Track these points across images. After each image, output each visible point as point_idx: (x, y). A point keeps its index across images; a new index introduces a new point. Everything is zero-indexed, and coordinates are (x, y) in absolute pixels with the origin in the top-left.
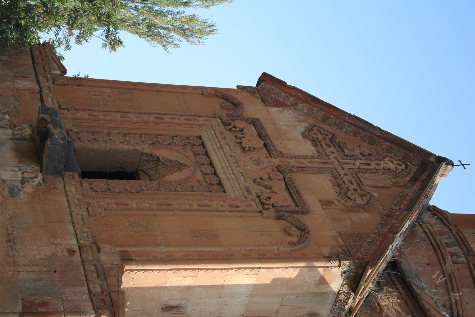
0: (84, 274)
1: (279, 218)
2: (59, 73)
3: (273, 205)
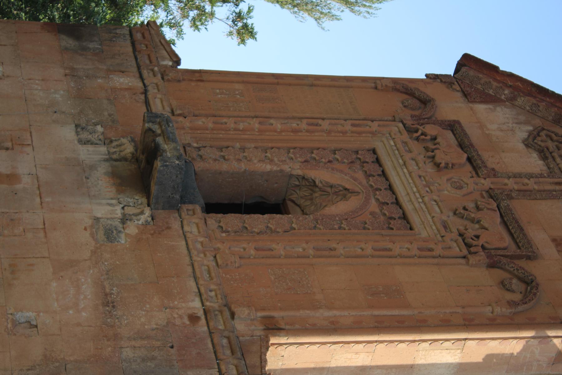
0: (212, 350)
1: (492, 266)
2: (170, 63)
3: (483, 247)
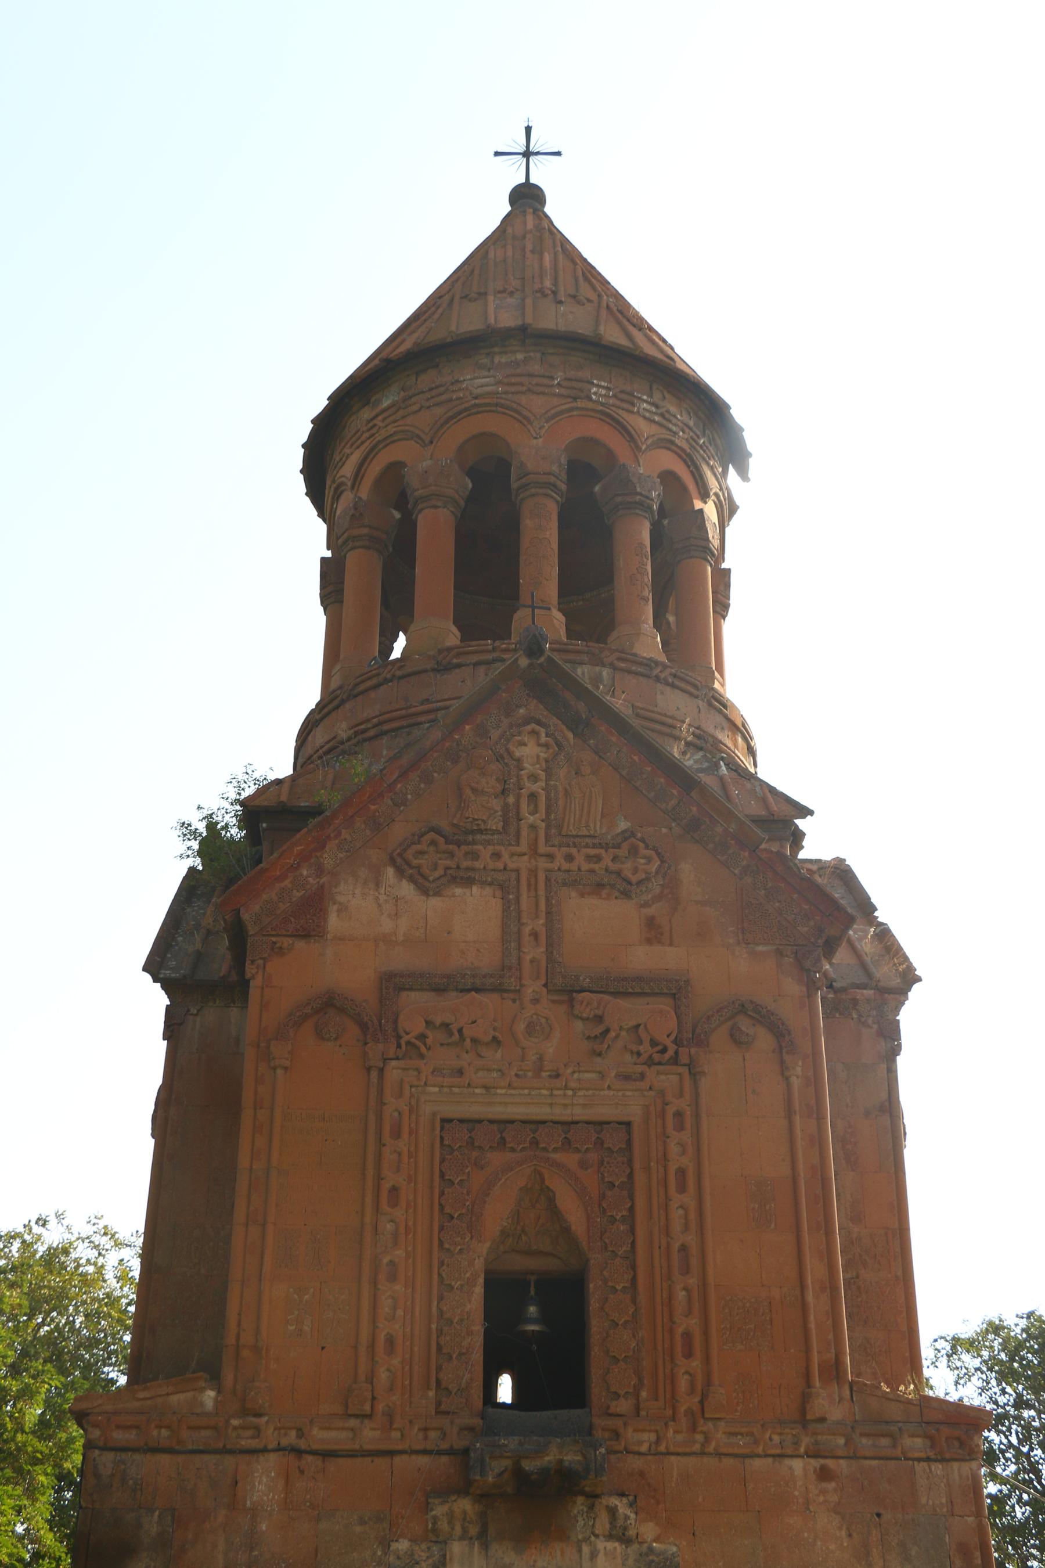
0: (882, 1462)
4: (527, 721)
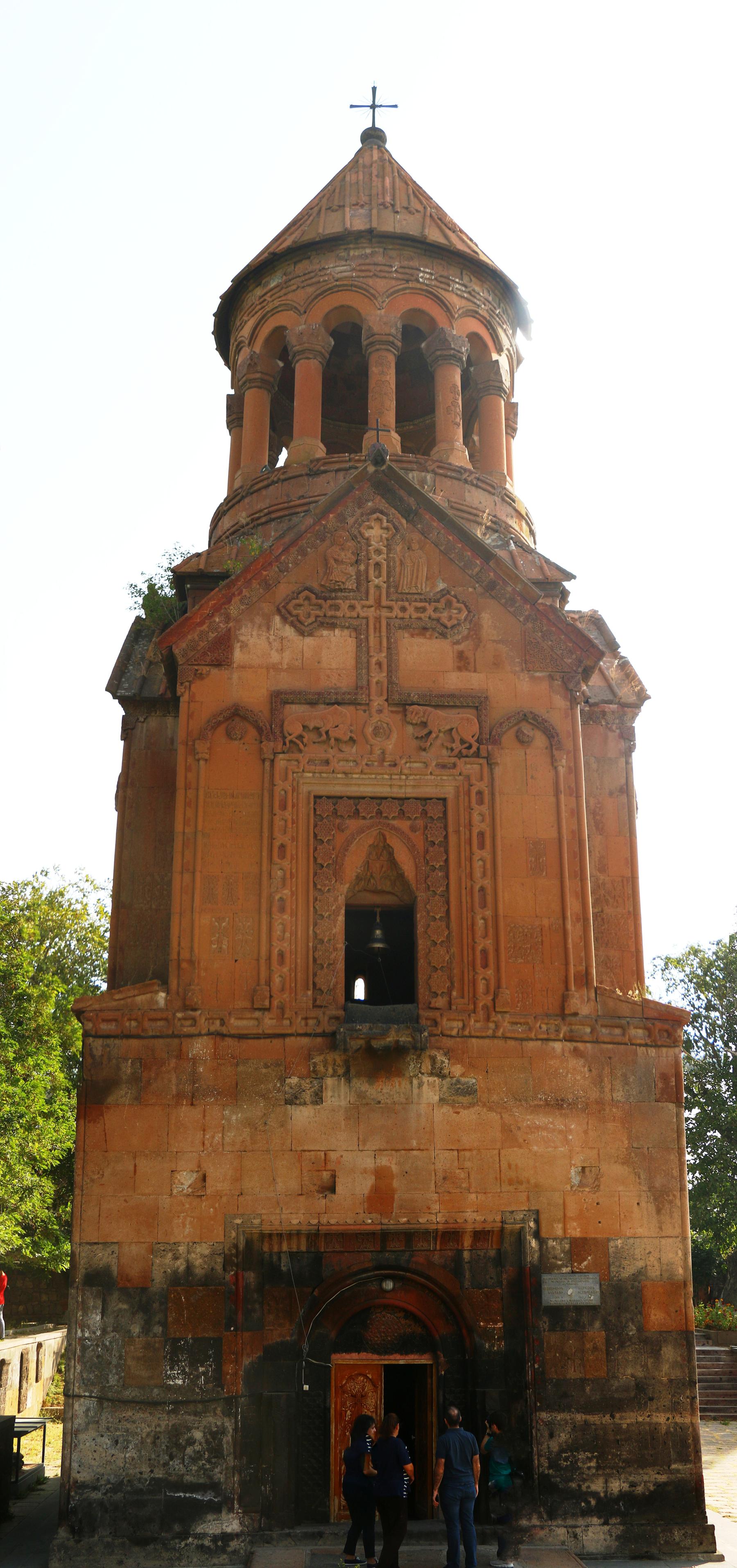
4: (374, 511)
